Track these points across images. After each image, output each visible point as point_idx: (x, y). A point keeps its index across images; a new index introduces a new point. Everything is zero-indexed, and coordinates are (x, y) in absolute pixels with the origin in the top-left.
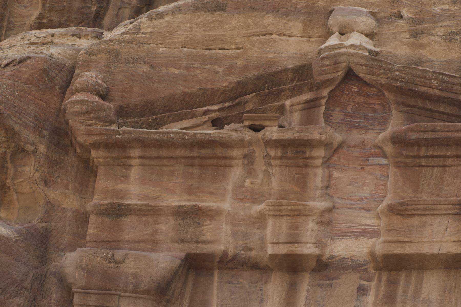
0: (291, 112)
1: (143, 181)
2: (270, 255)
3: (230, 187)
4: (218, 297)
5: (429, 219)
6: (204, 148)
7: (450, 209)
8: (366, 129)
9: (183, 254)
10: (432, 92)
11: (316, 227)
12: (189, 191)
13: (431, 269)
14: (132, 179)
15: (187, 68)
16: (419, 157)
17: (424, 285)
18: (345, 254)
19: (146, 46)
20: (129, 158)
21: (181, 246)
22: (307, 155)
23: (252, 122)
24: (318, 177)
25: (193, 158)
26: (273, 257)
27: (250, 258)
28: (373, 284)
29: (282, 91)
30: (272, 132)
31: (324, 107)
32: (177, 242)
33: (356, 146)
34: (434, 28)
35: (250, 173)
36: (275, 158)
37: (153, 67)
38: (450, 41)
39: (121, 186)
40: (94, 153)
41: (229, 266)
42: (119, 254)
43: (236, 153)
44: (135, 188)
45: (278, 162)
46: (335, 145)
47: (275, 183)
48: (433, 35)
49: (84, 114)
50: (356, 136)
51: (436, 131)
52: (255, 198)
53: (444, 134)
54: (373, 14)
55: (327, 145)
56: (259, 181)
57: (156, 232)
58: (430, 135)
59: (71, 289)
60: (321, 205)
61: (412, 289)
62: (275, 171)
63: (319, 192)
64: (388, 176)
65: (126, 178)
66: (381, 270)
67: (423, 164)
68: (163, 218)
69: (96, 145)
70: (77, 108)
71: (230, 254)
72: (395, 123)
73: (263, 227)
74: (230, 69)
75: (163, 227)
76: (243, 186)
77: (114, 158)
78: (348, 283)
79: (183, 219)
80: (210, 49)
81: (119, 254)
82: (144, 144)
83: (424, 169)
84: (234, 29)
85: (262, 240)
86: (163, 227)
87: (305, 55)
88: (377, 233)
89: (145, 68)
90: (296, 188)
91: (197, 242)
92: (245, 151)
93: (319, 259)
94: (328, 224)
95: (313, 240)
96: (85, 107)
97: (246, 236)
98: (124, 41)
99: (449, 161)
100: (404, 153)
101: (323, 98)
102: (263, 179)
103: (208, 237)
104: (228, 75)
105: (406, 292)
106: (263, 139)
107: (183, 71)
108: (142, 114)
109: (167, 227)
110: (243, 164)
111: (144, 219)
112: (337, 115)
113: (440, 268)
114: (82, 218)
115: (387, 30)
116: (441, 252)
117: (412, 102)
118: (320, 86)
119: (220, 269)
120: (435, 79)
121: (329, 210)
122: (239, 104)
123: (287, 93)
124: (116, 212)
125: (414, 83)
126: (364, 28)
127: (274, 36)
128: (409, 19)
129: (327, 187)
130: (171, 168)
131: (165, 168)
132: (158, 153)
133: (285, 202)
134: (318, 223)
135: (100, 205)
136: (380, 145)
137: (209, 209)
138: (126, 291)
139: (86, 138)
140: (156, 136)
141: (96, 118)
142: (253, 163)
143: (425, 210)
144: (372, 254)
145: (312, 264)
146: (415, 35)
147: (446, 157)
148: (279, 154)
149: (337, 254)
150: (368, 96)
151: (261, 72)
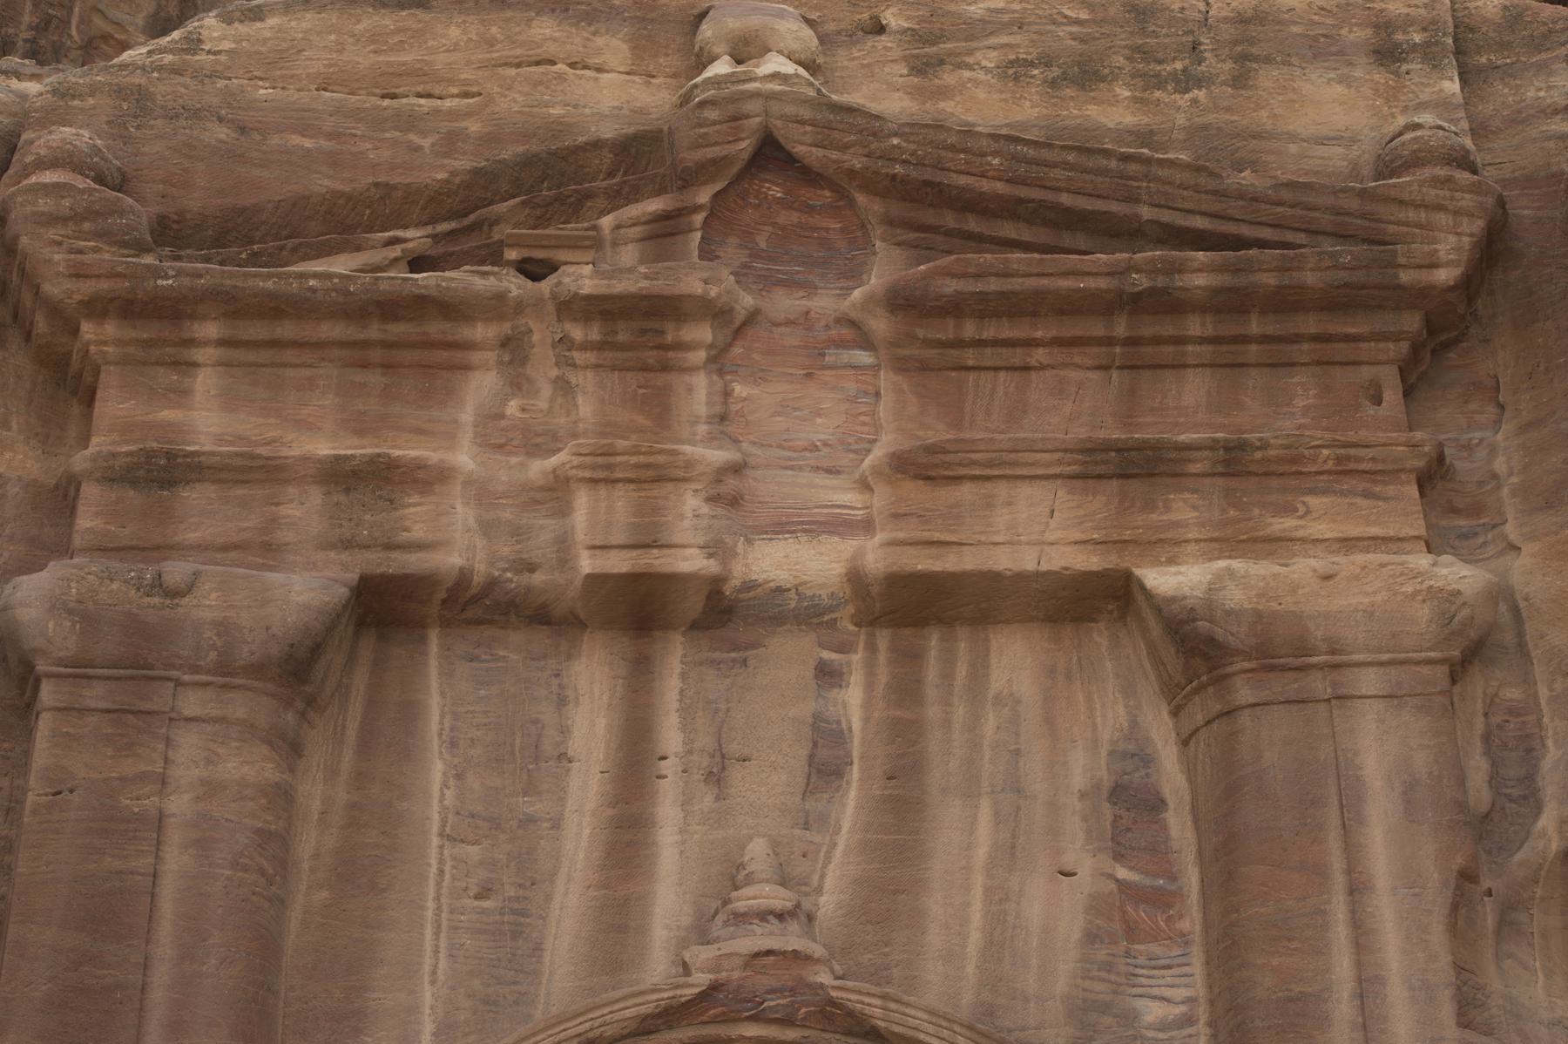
0: (615, 244)
1: (229, 401)
2: (588, 576)
3: (467, 416)
4: (443, 694)
5: (1002, 490)
6: (396, 318)
7: (1060, 462)
8: (810, 288)
9: (353, 577)
10: (986, 186)
11: (705, 509)
12: (361, 427)
13: (1007, 622)
14: (199, 396)
15: (335, 136)
16: (959, 344)
17: (993, 660)
18: (782, 576)
19: (221, 84)
20: (190, 343)
21: (345, 556)
22: (669, 338)
23: (526, 253)
24: (697, 393)
25: (365, 344)
26: (595, 580)
27: (528, 589)
28: (857, 658)
29: (589, 195)
30: (580, 277)
31: (699, 234)
32: (331, 546)
33: (789, 323)
34: (970, 52)
35: (518, 384)
36: (584, 347)
37: (243, 130)
38: (1016, 78)
39: (167, 414)
40: (88, 330)
41: (469, 614)
42: (176, 571)
43: (481, 332)
44: (207, 417)
45: (591, 357)
46: (740, 316)
47: (586, 408)
48: (970, 68)
49: (64, 220)
50: (784, 303)
51: (1007, 275)
52: (536, 443)
53: (1031, 283)
54: (810, 23)
55: (717, 312)
56: (543, 404)
57: (274, 521)
58: (993, 285)
59: (30, 667)
60: (718, 456)
61: (962, 671)
62: (585, 380)
63: (702, 429)
64: (878, 394)
65: (181, 395)
66: (872, 624)
67: (970, 363)
68: (292, 490)
69: (97, 308)
70: (44, 204)
71: (478, 579)
72: (885, 268)
73: (564, 511)
74: (451, 142)
75: (292, 511)
76: (502, 416)
77: (148, 344)
78: (788, 658)
79: (347, 491)
80: (394, 97)
81: (176, 571)
82: (234, 306)
83: (972, 376)
84: (455, 48)
85: (564, 544)
86: (292, 511)
87: (641, 111)
88: (867, 526)
89: (223, 133)
90: (641, 420)
91: (390, 547)
92: (506, 328)
93: (714, 587)
94: (734, 502)
95: (701, 540)
96: (66, 203)
97: (518, 533)
98: (160, 68)
99: (1040, 355)
100: (921, 333)
101: (697, 208)
102: (552, 400)
103: (418, 532)
104: (447, 155)
105: (947, 676)
106: (554, 296)
107: (325, 144)
108: (220, 241)
109: (304, 511)
110: (500, 363)
111: (240, 491)
112: (732, 252)
113: (1031, 619)
114: (61, 498)
115: (844, 60)
116: (1044, 567)
117: (930, 217)
118: (688, 179)
119: (446, 624)
120: (995, 154)
121: (737, 469)
122: (476, 227)
123: (601, 202)
124: (162, 471)
125: (939, 166)
126: (795, 46)
127: (561, 67)
128: (905, 31)
129: (723, 418)
130: (308, 372)
131: (290, 373)
132: (270, 331)
133: (622, 444)
134: (708, 500)
135: (114, 455)
136: (853, 315)
137: (420, 465)
138: (195, 669)
139: (68, 285)
140: (269, 284)
141: (98, 235)
142: (524, 361)
143: (990, 464)
144: (855, 577)
145: (694, 605)
146: (922, 67)
147: (1030, 343)
148: (595, 334)
149: (761, 577)
150: (811, 210)
151: (534, 147)
